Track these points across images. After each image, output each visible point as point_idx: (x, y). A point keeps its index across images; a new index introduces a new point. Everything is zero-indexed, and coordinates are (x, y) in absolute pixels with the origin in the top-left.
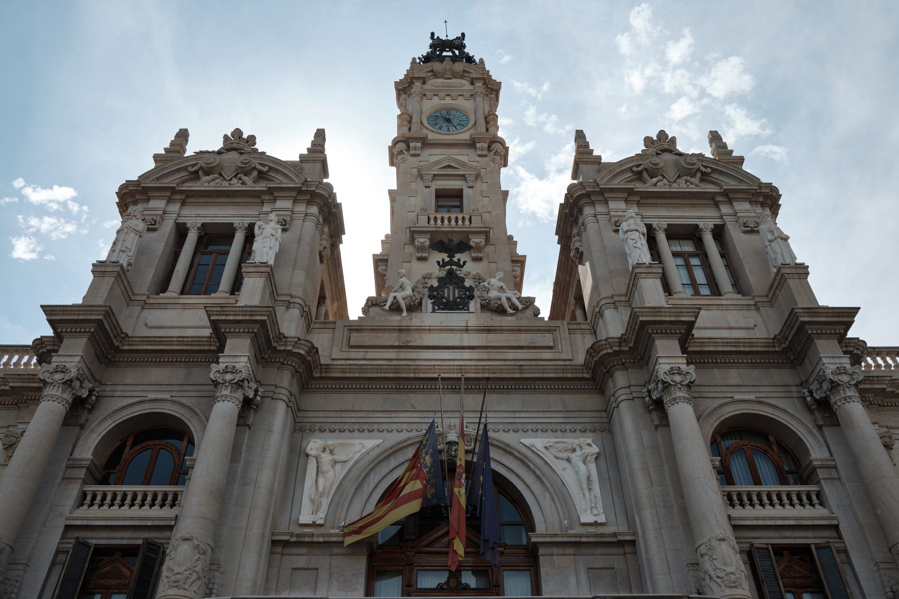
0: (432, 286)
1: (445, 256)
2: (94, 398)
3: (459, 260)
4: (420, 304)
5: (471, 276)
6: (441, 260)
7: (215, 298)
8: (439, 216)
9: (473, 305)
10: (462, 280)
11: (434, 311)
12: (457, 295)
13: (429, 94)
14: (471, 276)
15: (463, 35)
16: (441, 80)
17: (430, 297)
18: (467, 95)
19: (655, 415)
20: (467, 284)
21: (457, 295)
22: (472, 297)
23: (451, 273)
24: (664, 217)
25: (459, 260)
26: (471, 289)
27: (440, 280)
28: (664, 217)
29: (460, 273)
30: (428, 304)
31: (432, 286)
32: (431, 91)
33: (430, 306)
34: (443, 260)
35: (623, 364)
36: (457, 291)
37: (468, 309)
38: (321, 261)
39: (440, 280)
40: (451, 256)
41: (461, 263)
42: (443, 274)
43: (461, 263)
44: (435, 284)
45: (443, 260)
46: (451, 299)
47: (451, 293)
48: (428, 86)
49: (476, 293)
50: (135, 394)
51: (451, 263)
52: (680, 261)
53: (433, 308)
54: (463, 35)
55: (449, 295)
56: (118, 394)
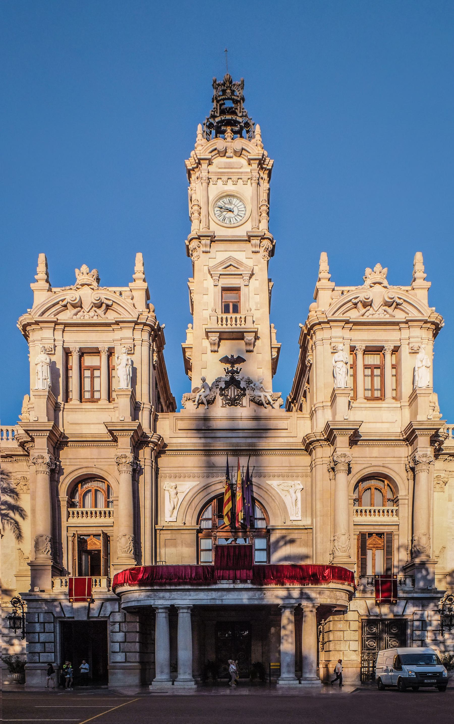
0: (221, 387)
1: (228, 366)
2: (58, 467)
3: (237, 369)
4: (215, 398)
5: (244, 380)
6: (226, 369)
7: (100, 405)
8: (224, 316)
9: (245, 401)
10: (239, 382)
11: (222, 407)
12: (236, 394)
13: (214, 178)
14: (244, 380)
15: (243, 82)
16: (224, 159)
17: (221, 395)
18: (245, 178)
19: (332, 473)
20: (243, 385)
21: (236, 394)
22: (244, 395)
23: (232, 378)
24: (364, 337)
25: (237, 369)
26: (244, 389)
27: (226, 382)
28: (364, 337)
29: (238, 377)
30: (219, 400)
31: (221, 387)
32: (216, 173)
33: (220, 401)
34: (228, 369)
35: (321, 445)
36: (236, 390)
37: (242, 404)
38: (154, 369)
39: (226, 382)
40: (232, 367)
41: (239, 371)
42: (228, 379)
43: (239, 371)
44: (223, 385)
45: (228, 369)
46: (233, 396)
47: (232, 392)
48: (212, 168)
49: (247, 392)
50: (76, 464)
51: (233, 372)
52: (368, 372)
53: (223, 404)
54: (243, 82)
55: (231, 394)
56: (68, 464)
